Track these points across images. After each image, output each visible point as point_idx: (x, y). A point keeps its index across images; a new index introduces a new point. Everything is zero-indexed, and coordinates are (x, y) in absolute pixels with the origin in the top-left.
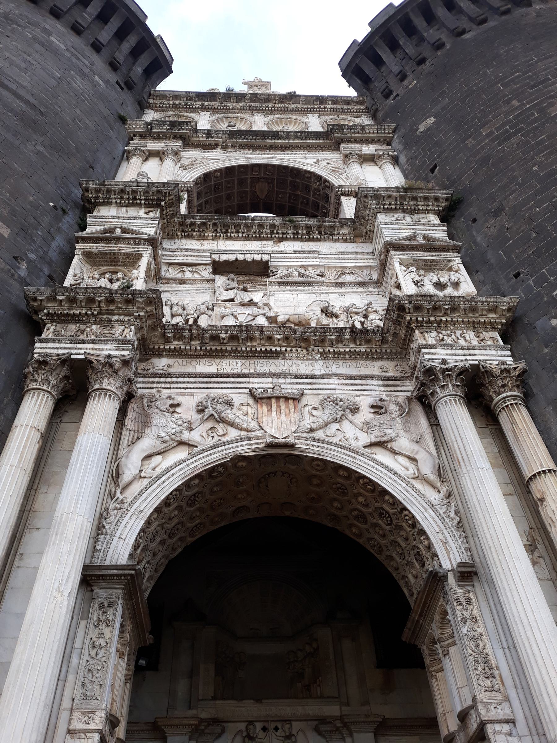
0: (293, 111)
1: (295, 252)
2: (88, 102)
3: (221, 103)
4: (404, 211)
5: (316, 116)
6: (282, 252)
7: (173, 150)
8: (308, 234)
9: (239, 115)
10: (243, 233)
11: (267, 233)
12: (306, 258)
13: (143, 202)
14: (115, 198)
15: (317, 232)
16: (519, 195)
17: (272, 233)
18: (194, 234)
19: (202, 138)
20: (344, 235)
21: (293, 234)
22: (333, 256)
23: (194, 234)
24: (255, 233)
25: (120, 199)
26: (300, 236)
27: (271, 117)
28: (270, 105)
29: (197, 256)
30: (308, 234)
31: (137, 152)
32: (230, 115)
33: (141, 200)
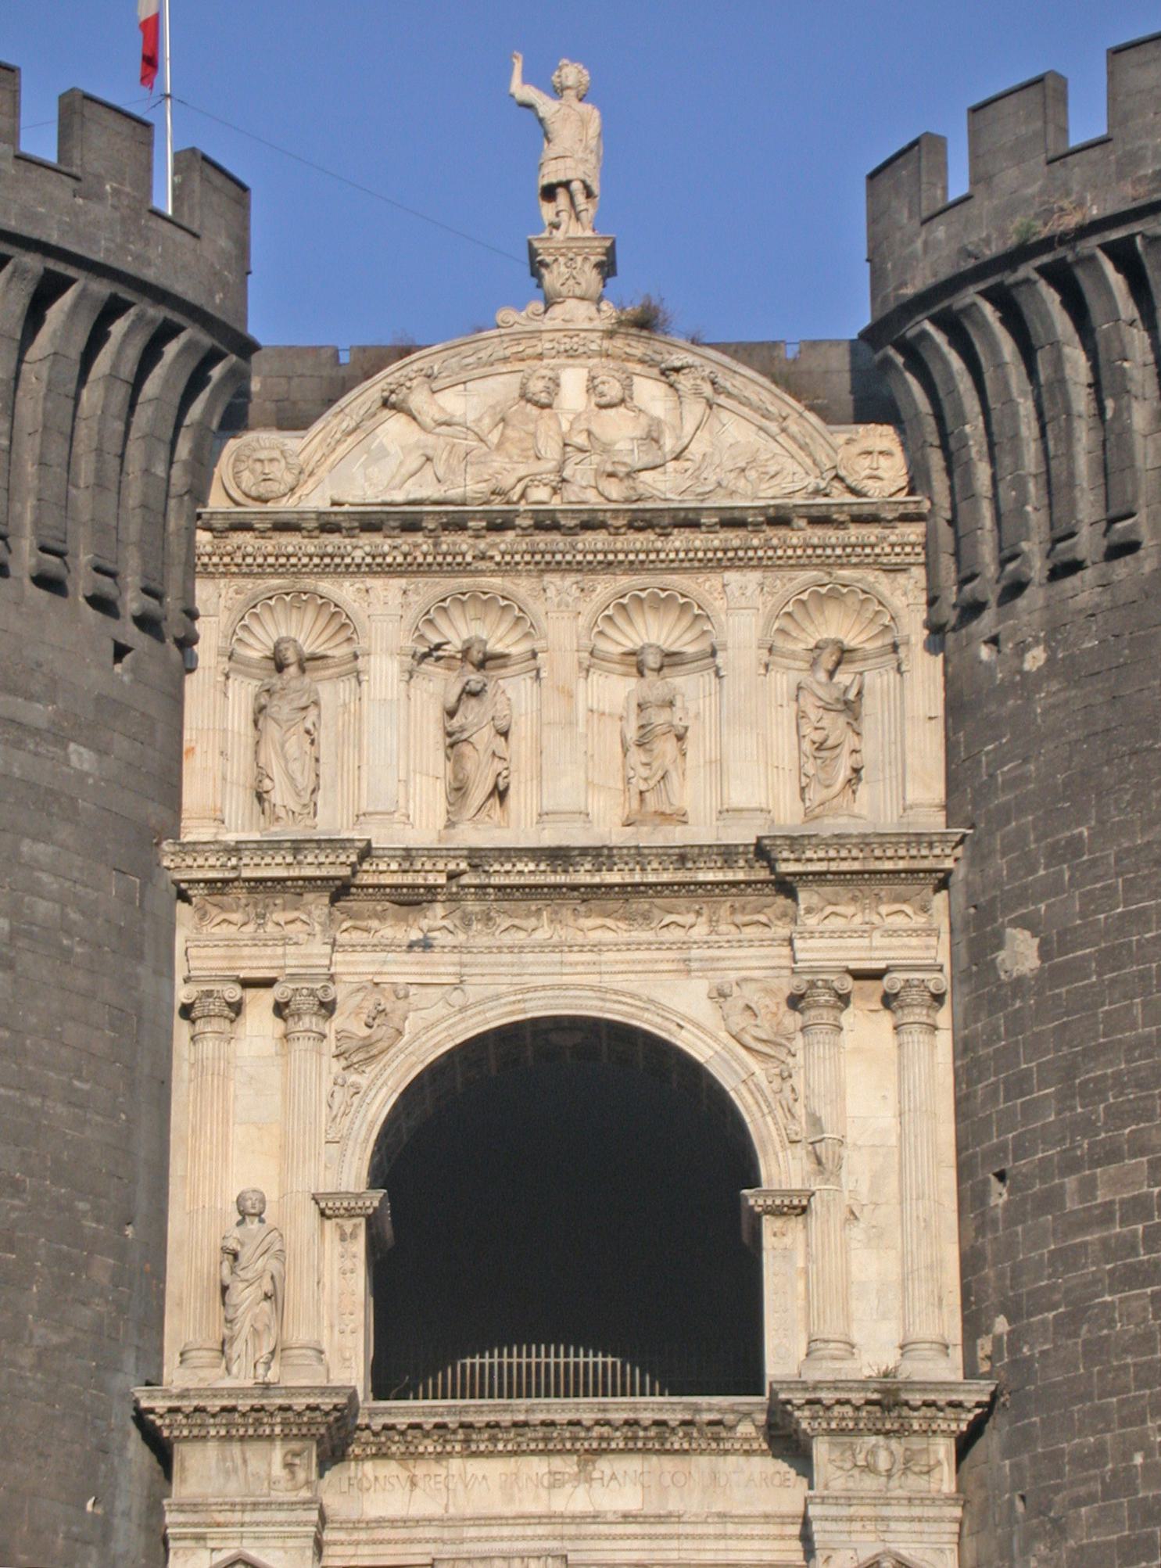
0: (672, 567)
1: (627, 1518)
2: (84, 941)
3: (436, 545)
4: (878, 1433)
5: (755, 576)
6: (595, 1518)
7: (312, 993)
8: (662, 1439)
9: (497, 581)
10: (507, 1441)
11: (563, 1440)
12: (651, 1537)
13: (278, 1430)
14: (215, 1425)
15: (681, 1434)
16: (1096, 1524)
17: (575, 1439)
18: (394, 1448)
19: (385, 873)
20: (746, 1440)
21: (626, 1439)
22: (711, 1530)
23: (394, 1448)
24: (535, 1440)
25: (226, 1425)
26: (640, 1445)
27: (606, 587)
28: (596, 540)
29: (404, 1542)
30: (662, 1439)
31: (215, 1007)
32: (465, 582)
33: (272, 1425)
